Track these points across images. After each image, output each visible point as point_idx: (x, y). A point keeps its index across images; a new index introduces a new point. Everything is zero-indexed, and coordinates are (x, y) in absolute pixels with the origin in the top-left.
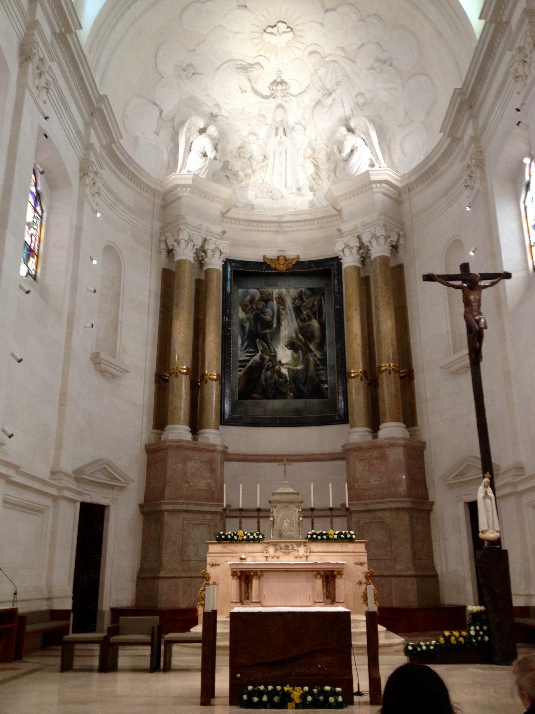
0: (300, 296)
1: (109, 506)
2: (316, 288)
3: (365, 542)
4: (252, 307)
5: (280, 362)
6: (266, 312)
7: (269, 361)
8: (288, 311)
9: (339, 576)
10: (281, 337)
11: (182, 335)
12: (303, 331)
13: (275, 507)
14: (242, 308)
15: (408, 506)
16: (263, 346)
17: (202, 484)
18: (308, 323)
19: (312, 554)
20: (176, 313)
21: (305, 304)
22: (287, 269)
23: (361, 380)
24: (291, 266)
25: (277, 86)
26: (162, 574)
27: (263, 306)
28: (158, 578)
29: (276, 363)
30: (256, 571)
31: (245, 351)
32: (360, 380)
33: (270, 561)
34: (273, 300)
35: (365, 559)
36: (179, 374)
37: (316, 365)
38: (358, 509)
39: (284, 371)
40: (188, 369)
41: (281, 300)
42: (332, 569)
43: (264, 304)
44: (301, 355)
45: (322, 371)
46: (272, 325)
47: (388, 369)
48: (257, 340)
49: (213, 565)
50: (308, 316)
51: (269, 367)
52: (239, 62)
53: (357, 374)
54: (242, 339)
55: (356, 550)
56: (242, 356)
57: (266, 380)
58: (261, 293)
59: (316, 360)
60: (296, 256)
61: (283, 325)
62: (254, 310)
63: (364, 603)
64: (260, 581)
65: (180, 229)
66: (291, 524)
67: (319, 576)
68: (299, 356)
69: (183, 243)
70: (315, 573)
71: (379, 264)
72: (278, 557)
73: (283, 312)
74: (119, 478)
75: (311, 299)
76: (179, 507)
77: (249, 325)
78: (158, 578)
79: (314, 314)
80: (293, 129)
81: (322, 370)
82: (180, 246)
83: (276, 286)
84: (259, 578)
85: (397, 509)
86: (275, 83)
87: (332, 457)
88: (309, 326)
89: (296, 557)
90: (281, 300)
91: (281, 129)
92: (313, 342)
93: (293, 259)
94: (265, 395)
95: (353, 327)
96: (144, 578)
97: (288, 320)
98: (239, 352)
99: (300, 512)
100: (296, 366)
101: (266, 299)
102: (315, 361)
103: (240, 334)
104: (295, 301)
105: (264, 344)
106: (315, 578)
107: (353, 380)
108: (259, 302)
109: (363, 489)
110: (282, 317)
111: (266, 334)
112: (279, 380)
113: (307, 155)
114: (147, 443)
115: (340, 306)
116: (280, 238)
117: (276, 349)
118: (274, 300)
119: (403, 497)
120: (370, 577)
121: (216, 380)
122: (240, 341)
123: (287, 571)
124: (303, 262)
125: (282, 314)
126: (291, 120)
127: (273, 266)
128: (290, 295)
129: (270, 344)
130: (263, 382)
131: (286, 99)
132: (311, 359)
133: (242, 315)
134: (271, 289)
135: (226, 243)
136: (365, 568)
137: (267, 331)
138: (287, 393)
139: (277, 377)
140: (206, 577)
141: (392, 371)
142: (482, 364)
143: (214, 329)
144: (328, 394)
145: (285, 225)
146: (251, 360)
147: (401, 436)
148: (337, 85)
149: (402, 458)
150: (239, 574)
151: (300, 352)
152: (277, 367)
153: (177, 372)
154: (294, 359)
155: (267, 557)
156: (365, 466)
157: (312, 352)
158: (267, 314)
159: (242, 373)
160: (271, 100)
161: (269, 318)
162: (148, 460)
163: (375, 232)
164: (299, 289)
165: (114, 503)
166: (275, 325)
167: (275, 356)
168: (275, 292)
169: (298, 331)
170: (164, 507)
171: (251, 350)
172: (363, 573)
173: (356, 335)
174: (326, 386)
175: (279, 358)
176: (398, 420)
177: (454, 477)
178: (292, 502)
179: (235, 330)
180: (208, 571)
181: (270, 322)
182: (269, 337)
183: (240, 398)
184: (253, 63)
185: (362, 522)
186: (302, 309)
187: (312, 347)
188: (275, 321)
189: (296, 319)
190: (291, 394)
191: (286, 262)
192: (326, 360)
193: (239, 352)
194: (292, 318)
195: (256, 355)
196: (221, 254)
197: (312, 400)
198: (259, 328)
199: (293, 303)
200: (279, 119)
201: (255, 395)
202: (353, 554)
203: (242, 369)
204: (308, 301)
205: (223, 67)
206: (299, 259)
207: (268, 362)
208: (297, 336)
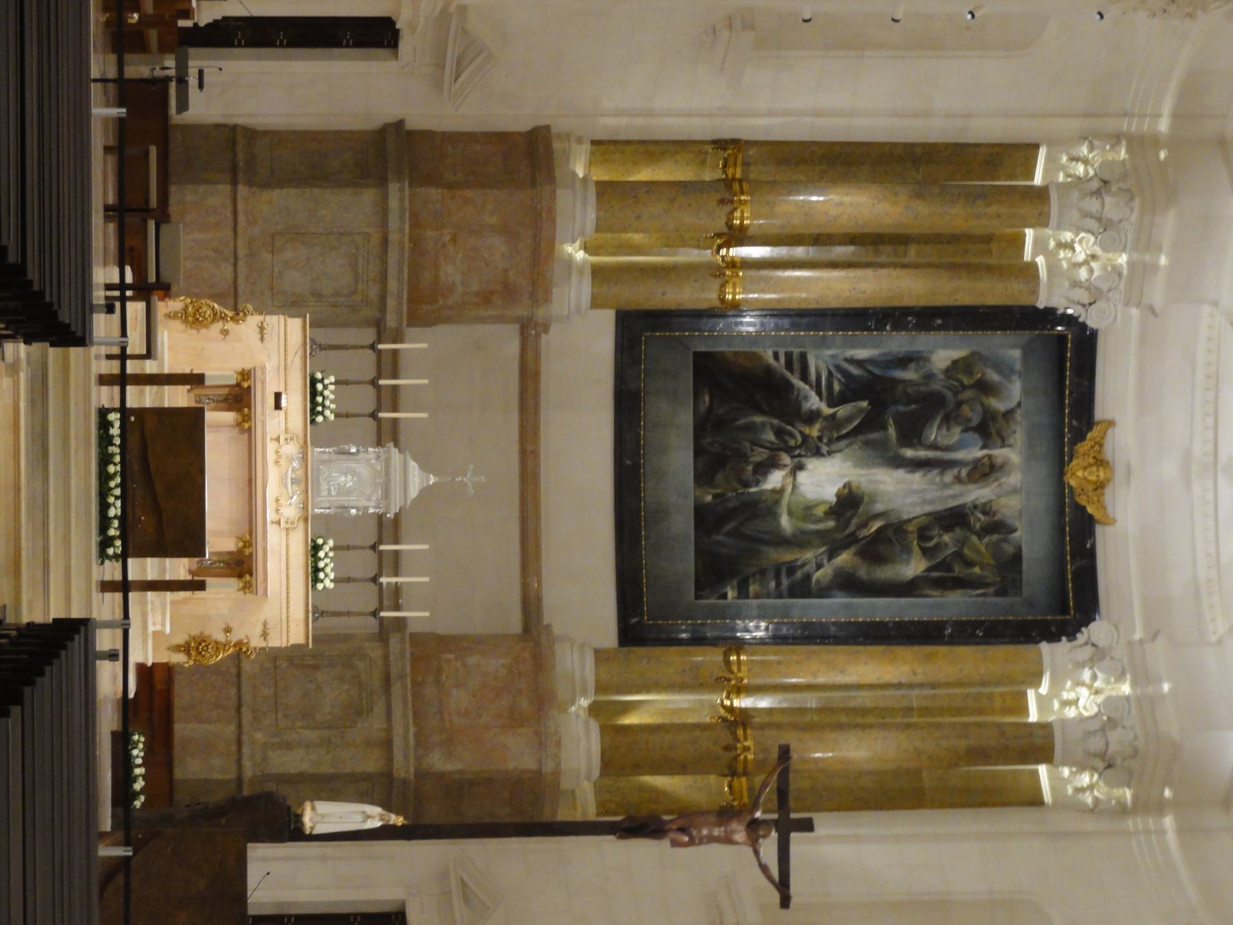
0: (998, 527)
1: (396, 57)
2: (1020, 572)
3: (308, 644)
4: (964, 387)
5: (800, 467)
6: (948, 429)
7: (805, 438)
9: (241, 585)
10: (875, 471)
11: (835, 213)
12: (890, 533)
13: (378, 458)
14: (964, 359)
15: (397, 770)
16: (849, 419)
17: (451, 272)
19: (284, 533)
20: (896, 194)
21: (974, 538)
22: (1071, 488)
24: (1082, 500)
26: (242, 190)
27: (969, 420)
28: (234, 183)
29: (800, 455)
30: (250, 419)
32: (719, 676)
33: (271, 447)
34: (984, 447)
35: (276, 641)
36: (728, 208)
37: (792, 569)
38: (392, 657)
39: (775, 479)
40: (742, 228)
41: (984, 471)
42: (254, 573)
43: (976, 421)
44: (821, 526)
45: (773, 584)
46: (910, 445)
47: (739, 745)
48: (865, 404)
49: (261, 328)
50: (937, 547)
51: (787, 438)
53: (735, 668)
54: (871, 361)
55: (292, 625)
57: (751, 428)
58: (1008, 415)
59: (806, 569)
60: (1111, 516)
61: (909, 476)
62: (956, 394)
63: (190, 636)
64: (230, 426)
65: (1132, 198)
66: (342, 491)
67: (241, 544)
68: (819, 521)
70: (248, 537)
71: (1031, 735)
72: (277, 462)
73: (949, 477)
74: (463, 77)
75: (988, 559)
76: (393, 222)
77: (909, 381)
78: (234, 183)
79: (944, 566)
81: (778, 585)
82: (1088, 199)
83: (1030, 457)
84: (238, 425)
85: (387, 744)
87: (531, 606)
88: (907, 550)
89: (277, 500)
90: (988, 471)
92: (857, 560)
93: (1103, 508)
94: (702, 427)
95: (866, 663)
96: (234, 142)
97: (925, 490)
98: (831, 352)
99: (366, 508)
100: (790, 513)
102: (804, 565)
103: (883, 354)
104: (984, 513)
105: (856, 423)
106: (238, 538)
107: (720, 658)
108: (979, 408)
109: (439, 671)
111: (884, 428)
112: (748, 463)
114: (554, 130)
115: (951, 635)
116: (1170, 469)
117: (838, 456)
118: (985, 452)
119: (418, 759)
120: (241, 651)
121: (723, 300)
122: (862, 354)
123: (250, 481)
124: (1091, 533)
125: (942, 473)
127: (1082, 447)
128: (999, 496)
129: (853, 439)
130: (742, 421)
132: (809, 555)
134: (1019, 443)
135: (1115, 319)
136: (256, 642)
137: (892, 431)
138: (713, 486)
139: (757, 459)
140: (238, 314)
141: (733, 754)
142: (611, 838)
143: (865, 292)
144: (708, 598)
145: (1210, 484)
146: (807, 387)
147: (564, 766)
149: (511, 766)
150: (245, 385)
151: (831, 524)
152: (786, 459)
153: (732, 202)
154: (809, 508)
155: (278, 439)
156: (496, 678)
157: (830, 559)
158: (944, 431)
159: (771, 361)
161: (933, 437)
162: (513, 133)
163: (1123, 727)
164: (1018, 524)
165: (403, 68)
166: (909, 453)
167: (818, 453)
168: (1011, 454)
169: (893, 518)
170: (393, 187)
171: (837, 387)
172: (246, 636)
173: (842, 672)
174: (731, 594)
175: (813, 464)
177: (462, 881)
178: (387, 493)
179: (897, 342)
180: (249, 318)
181: (920, 440)
183: (698, 356)
185: (361, 665)
187: (844, 558)
188: (923, 454)
189: (929, 514)
190: (709, 498)
191: (1090, 488)
193: (831, 352)
194: (931, 502)
195: (821, 399)
196: (1084, 306)
197: (692, 554)
198: (901, 408)
199: (975, 507)
201: (707, 399)
202: (284, 617)
203: (782, 360)
204: (983, 549)
206: (1104, 524)
207: (801, 433)
208: (876, 516)
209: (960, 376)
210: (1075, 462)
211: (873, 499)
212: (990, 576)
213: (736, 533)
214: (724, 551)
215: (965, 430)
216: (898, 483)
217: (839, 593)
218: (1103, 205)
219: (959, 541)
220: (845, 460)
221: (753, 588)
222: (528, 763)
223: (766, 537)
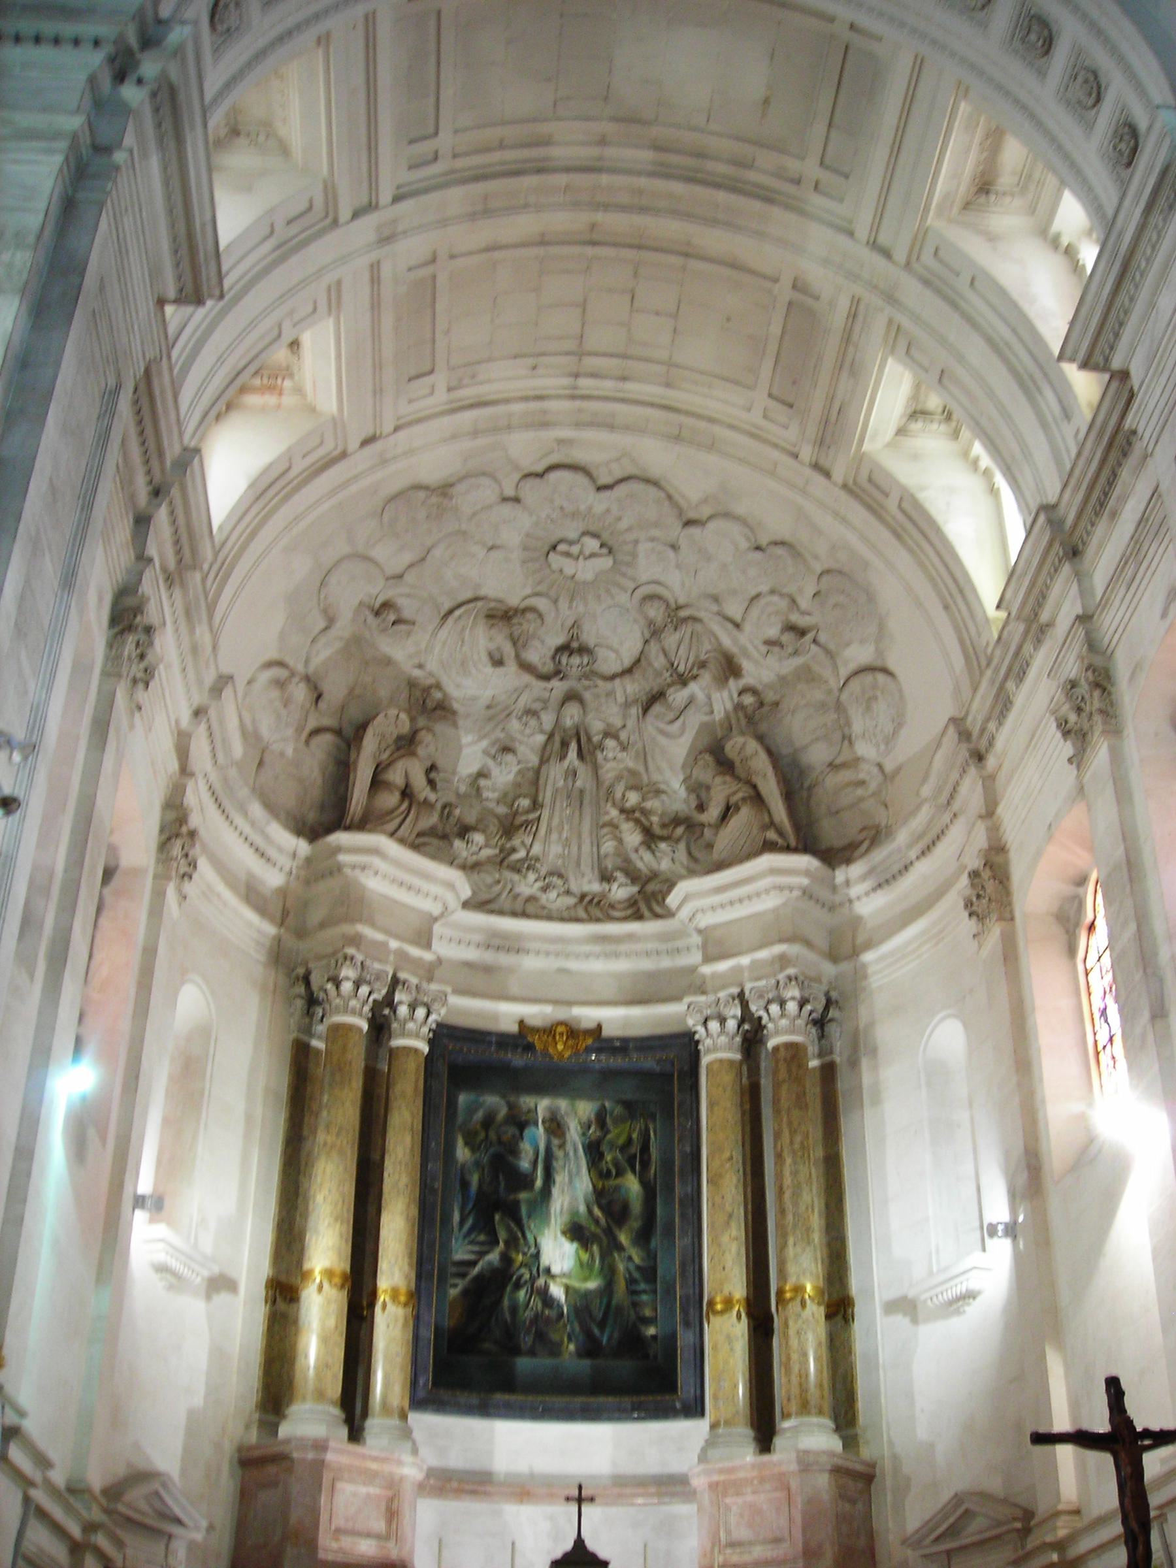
5: (548, 1271)
8: (571, 1153)
12: (604, 1202)
14: (464, 1138)
16: (509, 1230)
18: (619, 1181)
21: (609, 1136)
23: (739, 1317)
25: (570, 655)
27: (514, 1136)
31: (466, 1241)
34: (536, 1124)
37: (631, 1281)
39: (557, 1291)
41: (556, 1126)
43: (511, 1131)
45: (645, 1297)
46: (533, 1182)
48: (497, 1217)
50: (616, 1164)
52: (492, 605)
56: (461, 1252)
58: (511, 1107)
61: (557, 1185)
69: (347, 987)
73: (559, 1154)
77: (480, 1180)
79: (631, 1161)
80: (600, 747)
81: (645, 1292)
86: (565, 649)
88: (617, 1188)
91: (573, 746)
92: (626, 1227)
93: (588, 1032)
97: (570, 1172)
100: (586, 1279)
101: (520, 1122)
102: (630, 1273)
104: (589, 1127)
105: (512, 1225)
110: (556, 1164)
112: (543, 1312)
113: (628, 805)
117: (538, 1240)
122: (456, 1217)
124: (610, 1040)
126: (596, 726)
127: (539, 1046)
128: (576, 1113)
131: (586, 683)
132: (621, 1267)
133: (462, 1153)
137: (523, 1196)
138: (562, 1341)
139: (540, 1305)
148: (699, 668)
151: (595, 1248)
152: (541, 1282)
154: (581, 1265)
160: (555, 683)
166: (539, 1183)
167: (537, 1256)
169: (592, 1198)
174: (651, 1331)
175: (545, 1260)
176: (820, 1412)
181: (526, 1176)
182: (524, 1211)
184: (523, 605)
186: (604, 1148)
187: (623, 1238)
189: (589, 1172)
191: (570, 1042)
192: (654, 1270)
199: (584, 1134)
200: (568, 723)
201: (486, 1345)
203: (457, 1281)
205: (457, 613)
208: (590, 1211)
209: (478, 1142)
210: (551, 1050)
211: (574, 1213)
212: (639, 1126)
213: (602, 1325)
214: (616, 1335)
215: (522, 1139)
216: (563, 1192)
217: (653, 1244)
218: (347, 979)
219: (611, 1149)
220: (543, 1234)
221: (648, 1312)
222: (823, 1481)
223: (605, 1300)
